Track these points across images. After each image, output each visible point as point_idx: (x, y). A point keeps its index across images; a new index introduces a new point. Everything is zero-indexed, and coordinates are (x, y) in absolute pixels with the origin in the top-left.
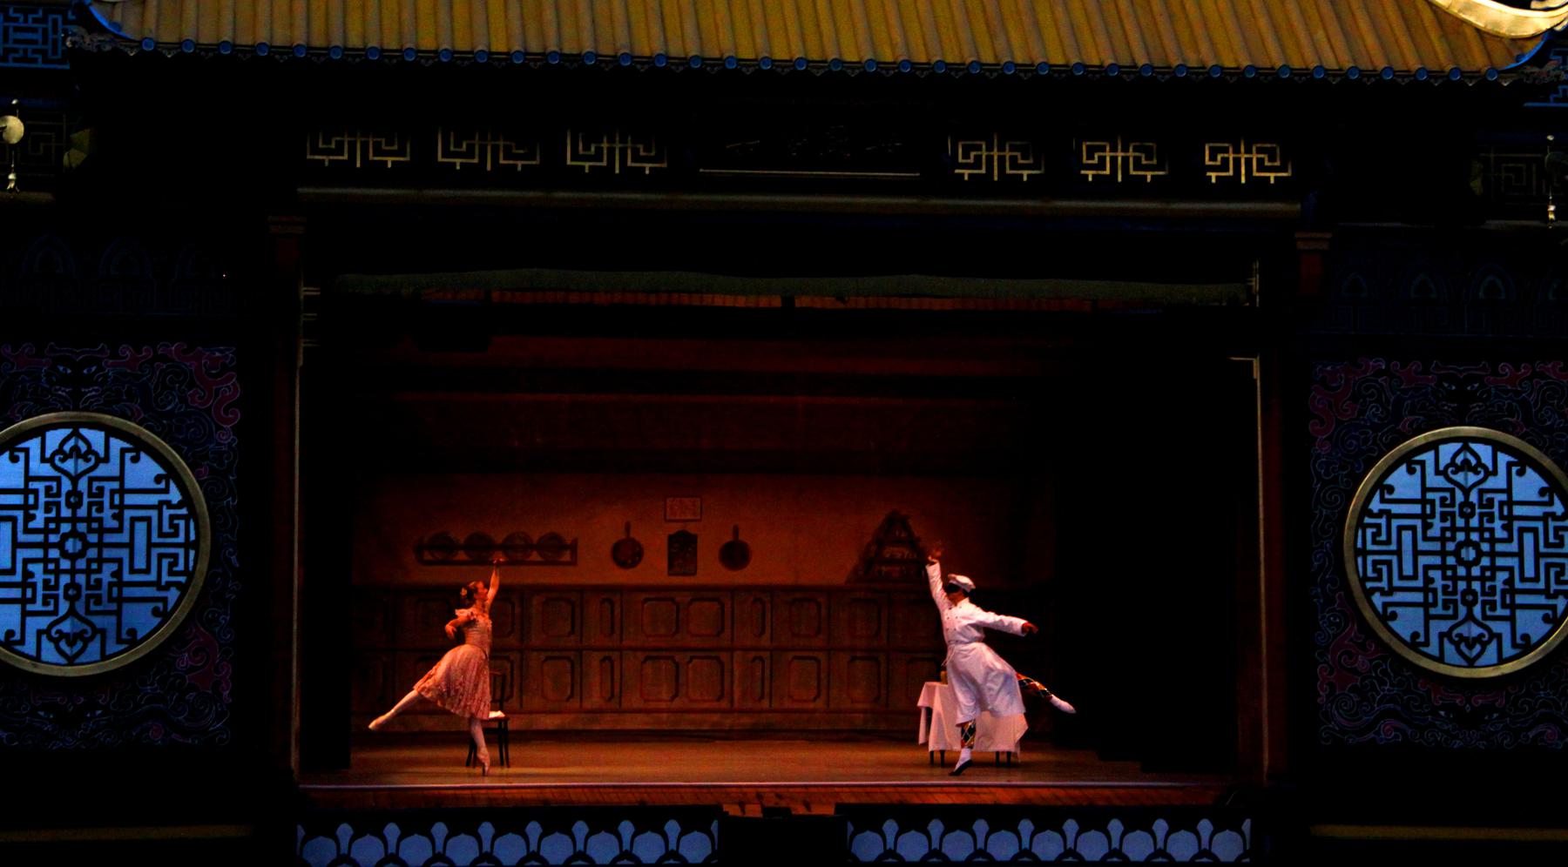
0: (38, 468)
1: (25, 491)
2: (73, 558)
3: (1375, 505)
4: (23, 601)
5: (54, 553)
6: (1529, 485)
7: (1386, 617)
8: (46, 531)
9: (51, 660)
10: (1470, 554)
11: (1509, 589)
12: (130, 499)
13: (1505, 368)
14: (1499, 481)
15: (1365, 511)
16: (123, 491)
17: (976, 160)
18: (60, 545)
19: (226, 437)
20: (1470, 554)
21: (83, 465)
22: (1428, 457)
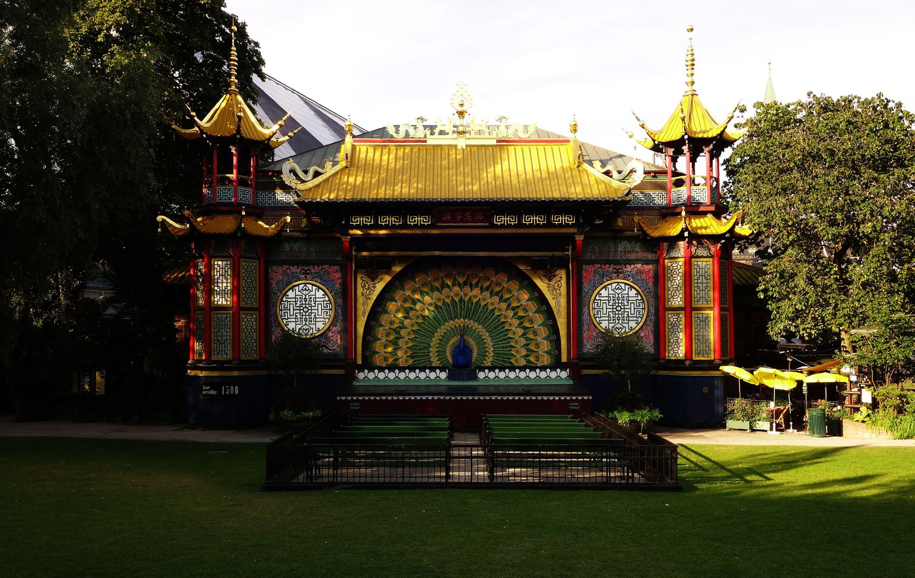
0: (298, 293)
3: (597, 298)
6: (633, 293)
7: (599, 324)
10: (619, 309)
14: (626, 292)
15: (595, 299)
17: (499, 220)
19: (338, 286)
20: (619, 309)
22: (610, 287)
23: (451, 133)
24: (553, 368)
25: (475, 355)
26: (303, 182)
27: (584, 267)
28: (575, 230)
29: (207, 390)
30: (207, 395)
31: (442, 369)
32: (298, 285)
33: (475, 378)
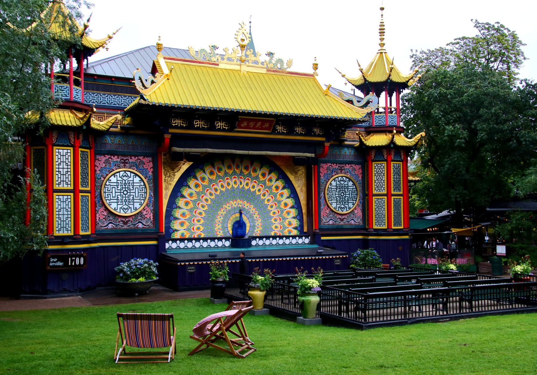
1: (117, 183)
2: (125, 195)
4: (117, 202)
5: (122, 194)
7: (331, 204)
8: (121, 190)
9: (122, 214)
10: (342, 194)
11: (348, 200)
12: (135, 184)
13: (347, 165)
16: (133, 183)
18: (123, 192)
19: (151, 173)
21: (127, 178)
23: (235, 61)
24: (300, 237)
25: (248, 228)
26: (146, 88)
27: (322, 165)
28: (323, 139)
29: (55, 262)
30: (54, 266)
31: (227, 239)
32: (119, 172)
33: (250, 245)
